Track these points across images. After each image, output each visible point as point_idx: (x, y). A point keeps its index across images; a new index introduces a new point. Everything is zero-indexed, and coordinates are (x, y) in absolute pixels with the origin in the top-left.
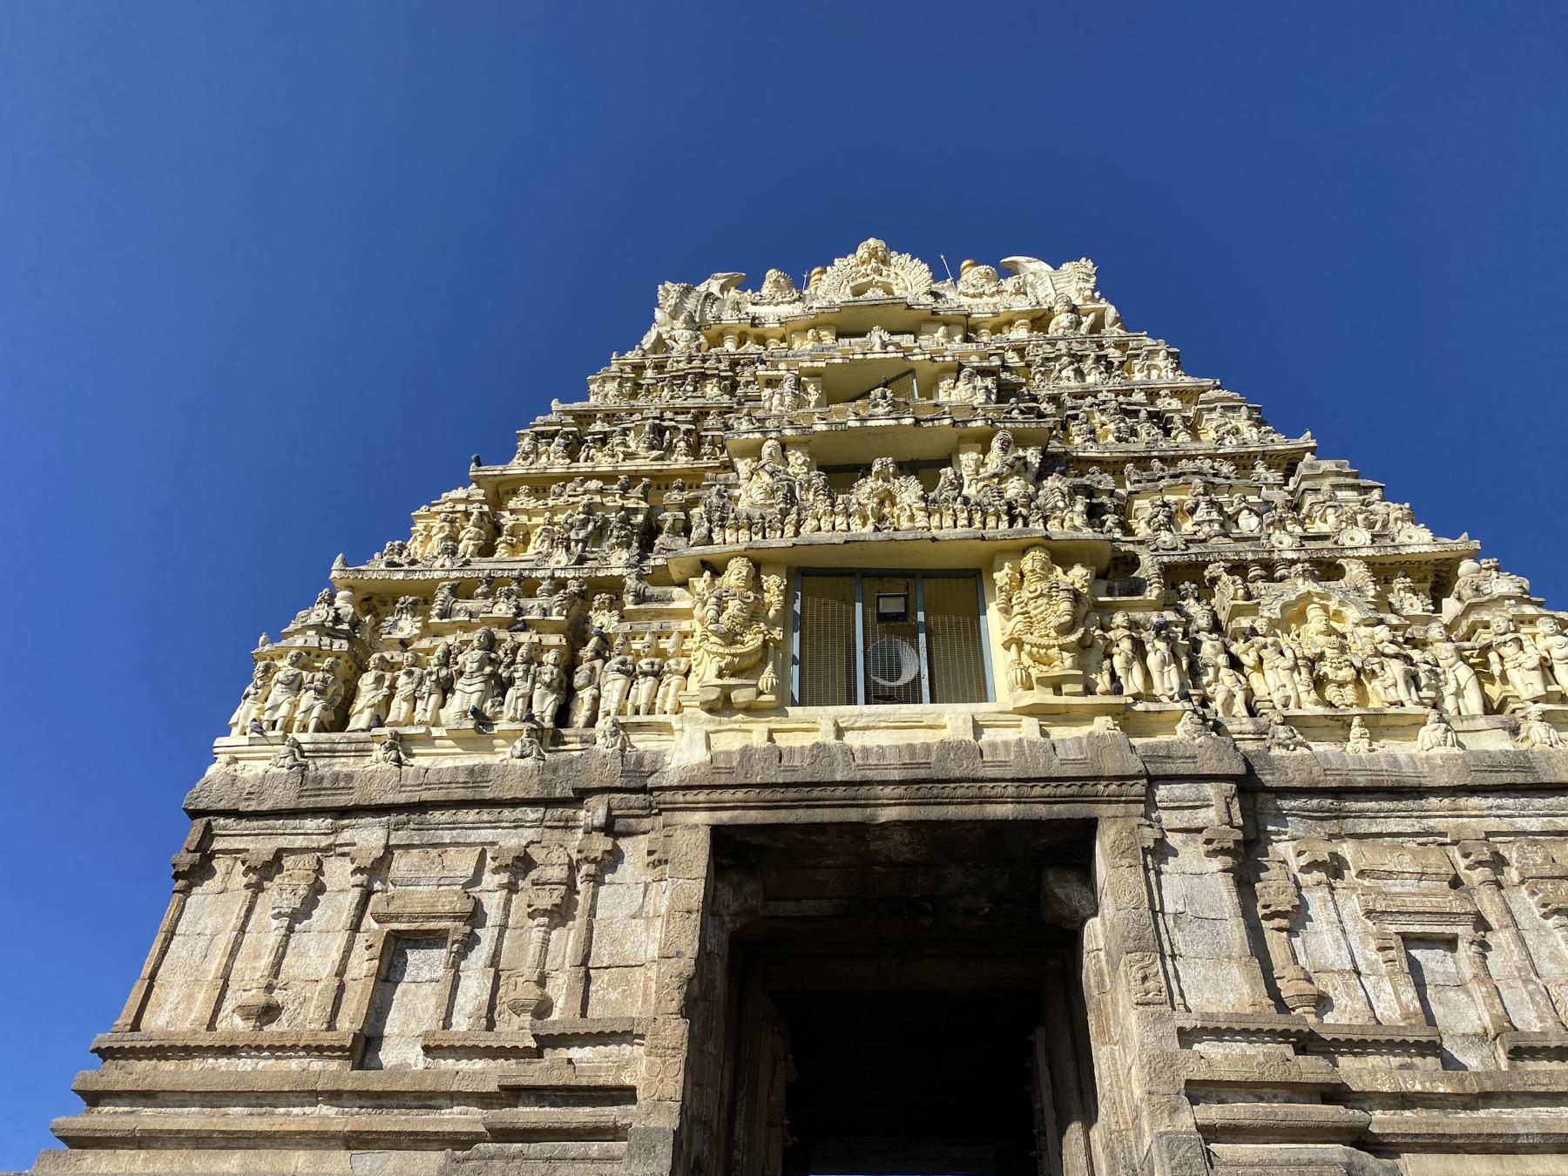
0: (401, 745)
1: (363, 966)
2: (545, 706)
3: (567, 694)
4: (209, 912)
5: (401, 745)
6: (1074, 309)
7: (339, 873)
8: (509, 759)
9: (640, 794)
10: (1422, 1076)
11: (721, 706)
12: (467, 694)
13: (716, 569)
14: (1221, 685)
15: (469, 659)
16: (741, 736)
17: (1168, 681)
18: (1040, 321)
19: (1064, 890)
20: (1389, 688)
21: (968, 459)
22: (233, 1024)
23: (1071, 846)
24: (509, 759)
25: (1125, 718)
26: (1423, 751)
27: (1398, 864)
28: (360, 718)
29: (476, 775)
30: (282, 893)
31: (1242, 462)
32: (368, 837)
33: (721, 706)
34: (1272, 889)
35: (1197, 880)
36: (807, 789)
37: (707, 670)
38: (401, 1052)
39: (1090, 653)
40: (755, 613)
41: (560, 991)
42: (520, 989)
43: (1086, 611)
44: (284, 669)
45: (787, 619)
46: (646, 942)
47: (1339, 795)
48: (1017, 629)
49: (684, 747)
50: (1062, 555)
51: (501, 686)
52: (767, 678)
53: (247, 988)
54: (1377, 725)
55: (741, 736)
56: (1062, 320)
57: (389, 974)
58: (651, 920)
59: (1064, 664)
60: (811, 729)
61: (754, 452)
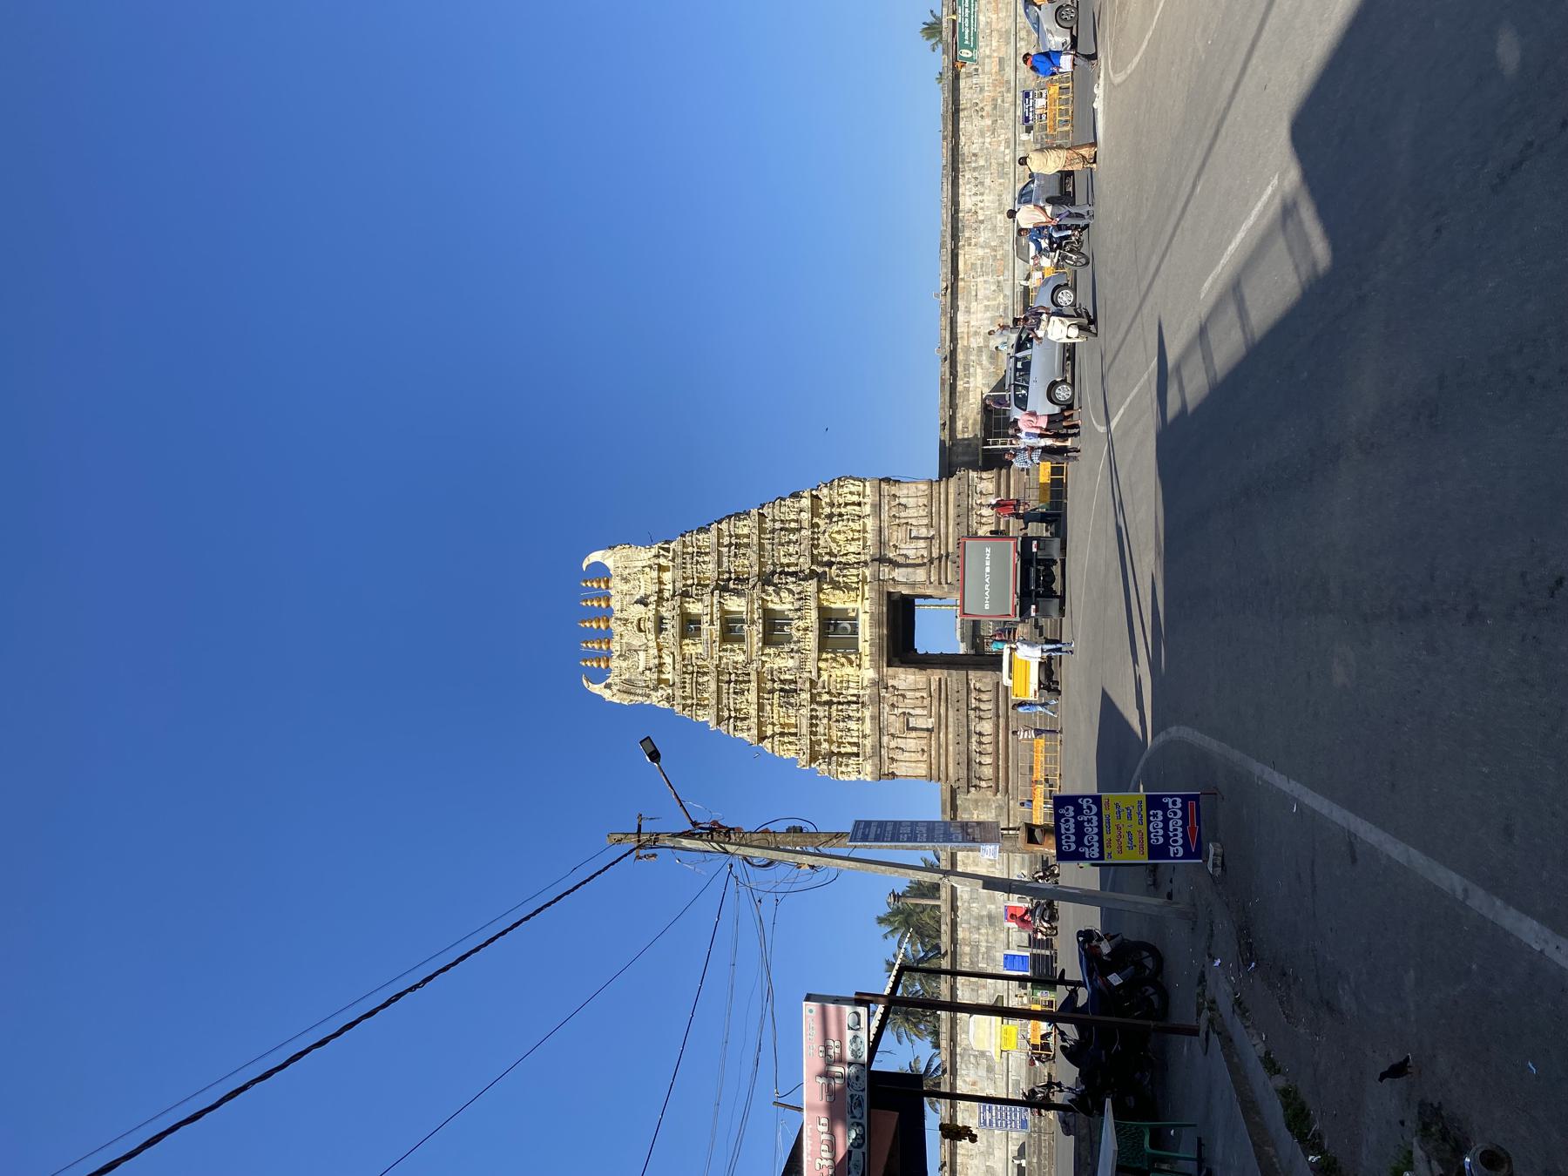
0: (864, 736)
1: (914, 734)
2: (854, 706)
3: (849, 703)
4: (901, 769)
5: (864, 736)
6: (657, 556)
7: (893, 744)
8: (867, 713)
9: (880, 683)
10: (936, 542)
11: (859, 666)
12: (852, 725)
13: (819, 669)
14: (852, 559)
15: (842, 724)
16: (866, 661)
17: (854, 572)
18: (661, 568)
19: (895, 597)
20: (856, 526)
21: (770, 605)
22: (925, 757)
23: (889, 594)
24: (867, 713)
25: (864, 581)
26: (870, 523)
27: (897, 536)
28: (855, 749)
29: (872, 718)
30: (898, 755)
31: (762, 531)
32: (885, 739)
33: (859, 666)
34: (900, 560)
35: (899, 574)
36: (880, 649)
37: (849, 670)
38: (930, 723)
39: (847, 588)
40: (834, 660)
41: (918, 694)
42: (918, 702)
43: (836, 586)
44: (843, 769)
45: (834, 652)
46: (911, 678)
47: (881, 543)
48: (837, 601)
49: (869, 674)
50: (820, 590)
51: (849, 717)
52: (853, 657)
53: (919, 756)
54: (865, 531)
55: (866, 661)
56: (662, 561)
57: (915, 729)
58: (906, 678)
59: (853, 594)
60: (864, 647)
61: (764, 662)
